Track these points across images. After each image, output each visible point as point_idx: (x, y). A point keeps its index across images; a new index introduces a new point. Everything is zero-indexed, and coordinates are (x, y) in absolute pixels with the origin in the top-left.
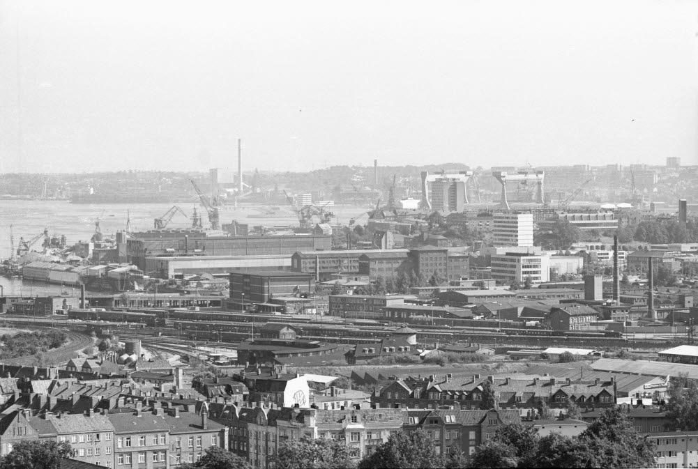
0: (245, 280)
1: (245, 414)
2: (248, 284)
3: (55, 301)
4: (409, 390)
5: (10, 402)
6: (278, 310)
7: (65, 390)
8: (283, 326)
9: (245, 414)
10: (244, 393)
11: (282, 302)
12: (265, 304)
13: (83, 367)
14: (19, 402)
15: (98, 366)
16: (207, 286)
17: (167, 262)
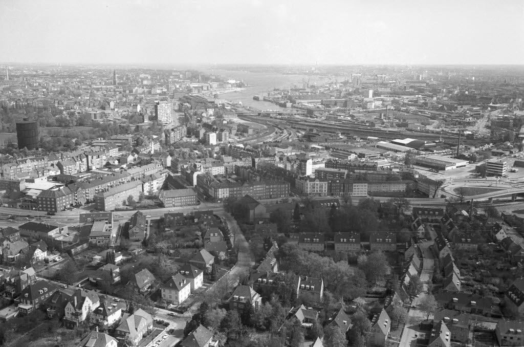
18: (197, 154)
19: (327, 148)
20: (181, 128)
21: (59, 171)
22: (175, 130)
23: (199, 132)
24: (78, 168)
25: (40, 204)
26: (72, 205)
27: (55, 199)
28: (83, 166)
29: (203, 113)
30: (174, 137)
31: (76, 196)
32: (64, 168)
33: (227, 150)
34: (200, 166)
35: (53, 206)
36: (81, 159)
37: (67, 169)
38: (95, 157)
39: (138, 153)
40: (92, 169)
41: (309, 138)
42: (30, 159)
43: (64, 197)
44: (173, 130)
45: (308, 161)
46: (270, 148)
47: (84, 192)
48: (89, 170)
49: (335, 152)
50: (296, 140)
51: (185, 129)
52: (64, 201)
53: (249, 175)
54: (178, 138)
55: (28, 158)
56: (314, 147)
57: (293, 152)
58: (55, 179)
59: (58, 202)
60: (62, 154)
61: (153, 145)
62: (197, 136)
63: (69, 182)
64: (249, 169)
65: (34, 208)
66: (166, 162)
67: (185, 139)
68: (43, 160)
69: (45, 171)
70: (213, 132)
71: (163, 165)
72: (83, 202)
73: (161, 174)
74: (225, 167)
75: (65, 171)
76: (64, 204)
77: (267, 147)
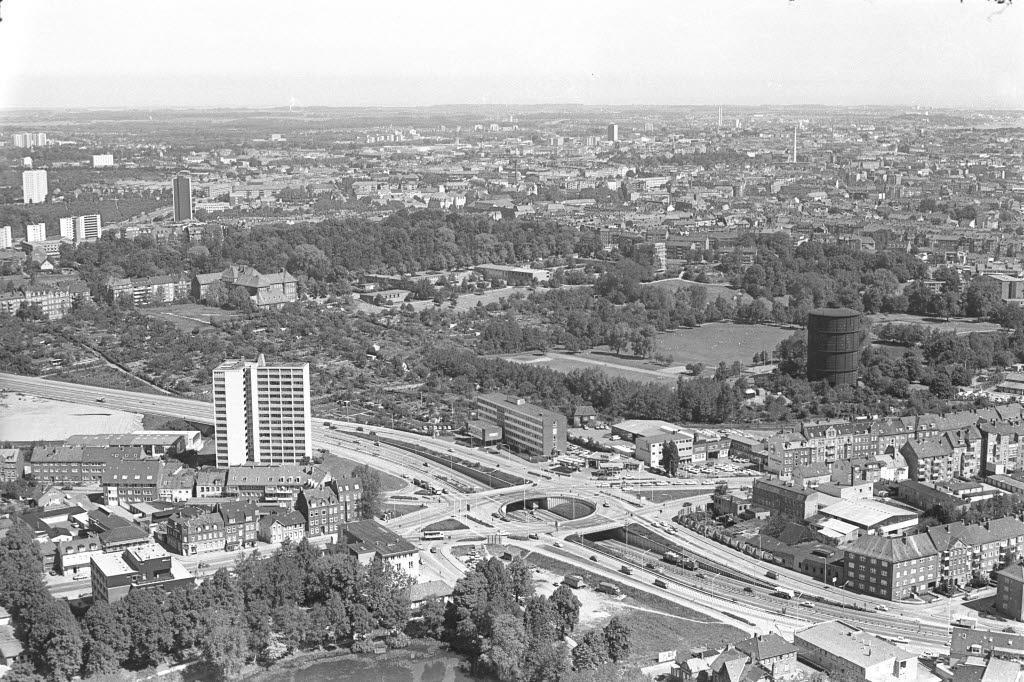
21: (907, 468)
24: (956, 466)
25: (851, 579)
26: (932, 584)
27: (891, 565)
28: (970, 461)
31: (947, 563)
32: (921, 462)
35: (884, 573)
36: (967, 441)
37: (928, 466)
38: (1005, 439)
40: (994, 473)
42: (834, 426)
43: (914, 562)
47: (969, 554)
48: (985, 472)
52: (913, 571)
55: (833, 422)
58: (894, 492)
59: (898, 575)
60: (917, 421)
63: (935, 512)
65: (835, 580)
68: (867, 433)
69: (870, 467)
72: (962, 578)
75: (921, 470)
76: (913, 581)
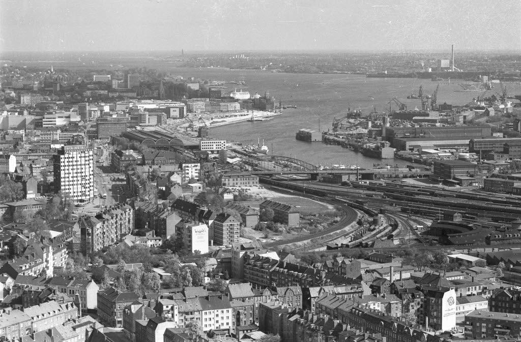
0: (442, 166)
1: (415, 334)
2: (442, 168)
3: (343, 177)
4: (510, 296)
5: (294, 313)
6: (458, 184)
7: (325, 297)
8: (456, 212)
9: (415, 334)
10: (422, 297)
11: (461, 180)
12: (451, 180)
13: (342, 263)
14: (299, 313)
15: (350, 263)
16: (424, 158)
17: (405, 142)
18: (161, 276)
19: (492, 261)
20: (119, 211)
22: (106, 216)
23: (164, 220)
29: (172, 173)
30: (103, 235)
33: (237, 266)
34: (172, 308)
39: (14, 275)
41: (444, 235)
44: (99, 217)
45: (445, 293)
46: (347, 261)
49: (513, 270)
50: (409, 240)
51: (130, 214)
53: (295, 329)
54: (114, 236)
56: (458, 259)
57: (406, 270)
61: (51, 254)
62: (160, 231)
64: (296, 317)
66: (84, 298)
67: (129, 240)
70: (200, 221)
71: (77, 305)
73: (74, 329)
74: (234, 310)
77: (340, 260)
